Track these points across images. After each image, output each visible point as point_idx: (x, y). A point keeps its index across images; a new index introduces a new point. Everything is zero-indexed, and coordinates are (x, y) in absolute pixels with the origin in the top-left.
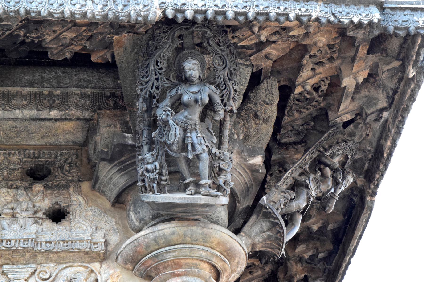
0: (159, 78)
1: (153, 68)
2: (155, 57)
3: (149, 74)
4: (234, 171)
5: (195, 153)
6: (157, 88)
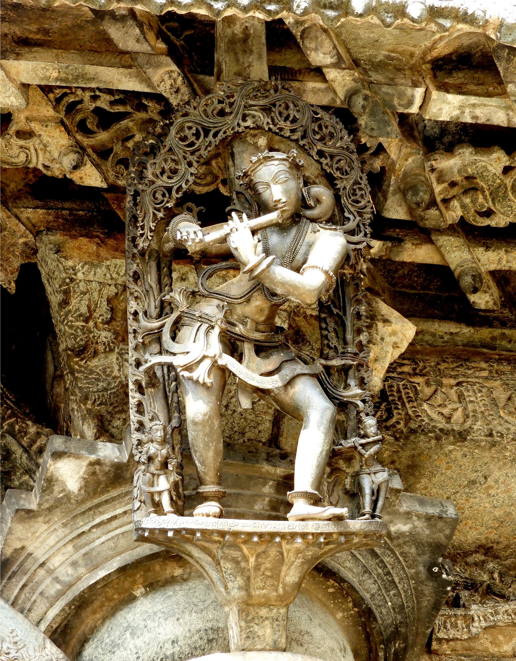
4: (84, 539)
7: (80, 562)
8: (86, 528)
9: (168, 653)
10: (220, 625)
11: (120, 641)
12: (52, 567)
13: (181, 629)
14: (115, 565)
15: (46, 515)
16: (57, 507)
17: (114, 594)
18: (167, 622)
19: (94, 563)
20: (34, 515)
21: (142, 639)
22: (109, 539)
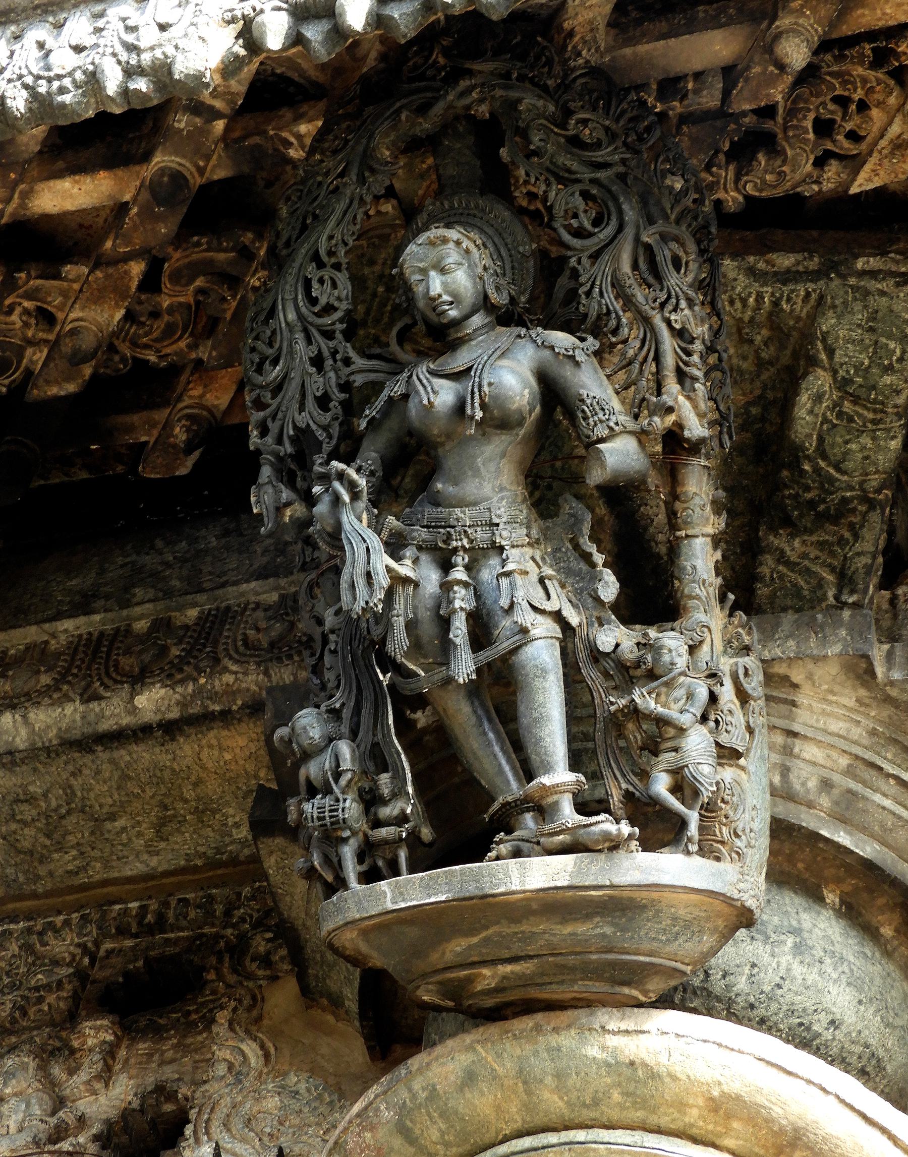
0: (326, 353)
1: (292, 316)
2: (296, 265)
3: (280, 348)
4: (869, 775)
5: (488, 655)
6: (323, 402)
7: (836, 792)
8: (889, 768)
9: (816, 1027)
10: (888, 1067)
11: (773, 935)
12: (796, 750)
13: (854, 1019)
14: (867, 849)
15: (875, 698)
16: (897, 708)
17: (802, 861)
18: (847, 989)
19: (848, 814)
20: (867, 682)
21: (805, 970)
22: (894, 814)
